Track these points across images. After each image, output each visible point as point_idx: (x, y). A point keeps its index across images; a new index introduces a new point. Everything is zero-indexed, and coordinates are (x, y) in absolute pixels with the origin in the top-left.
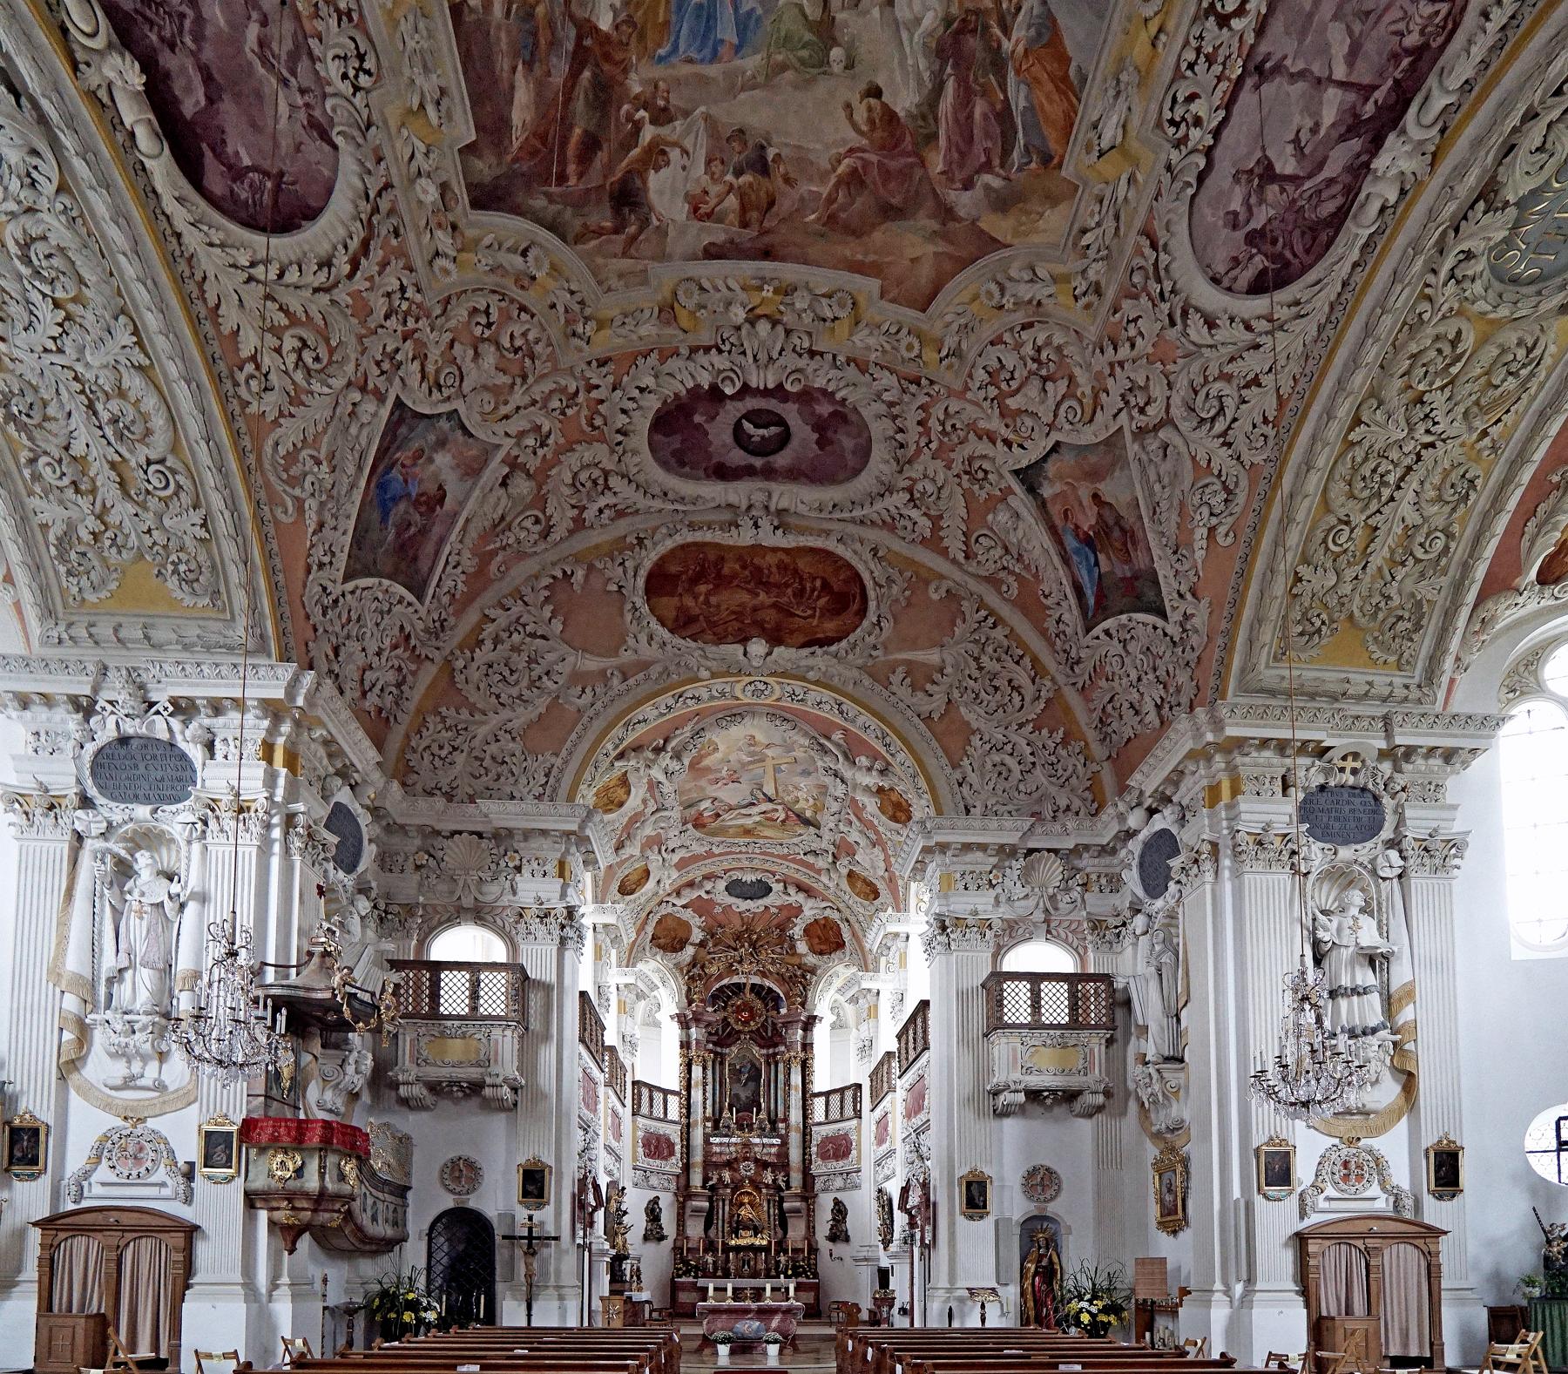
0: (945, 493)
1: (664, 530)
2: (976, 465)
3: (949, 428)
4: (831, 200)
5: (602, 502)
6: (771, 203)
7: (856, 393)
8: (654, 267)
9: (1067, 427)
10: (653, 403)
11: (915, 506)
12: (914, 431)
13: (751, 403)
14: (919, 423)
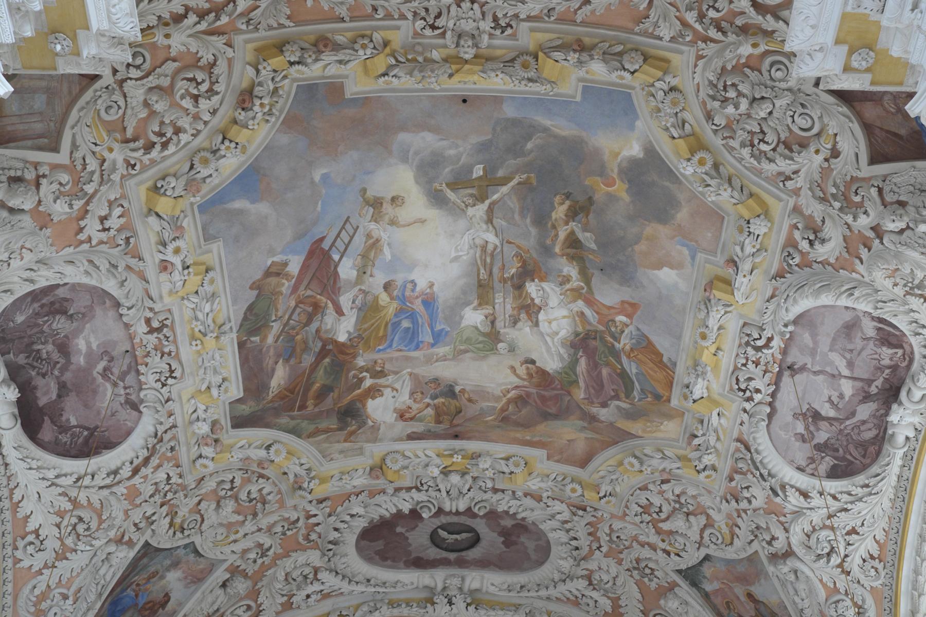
0: (619, 582)
1: (365, 608)
2: (643, 565)
3: (615, 539)
4: (503, 410)
5: (310, 589)
6: (459, 411)
7: (531, 512)
8: (368, 447)
9: (712, 545)
10: (360, 524)
11: (594, 589)
12: (584, 542)
13: (444, 520)
14: (590, 534)
